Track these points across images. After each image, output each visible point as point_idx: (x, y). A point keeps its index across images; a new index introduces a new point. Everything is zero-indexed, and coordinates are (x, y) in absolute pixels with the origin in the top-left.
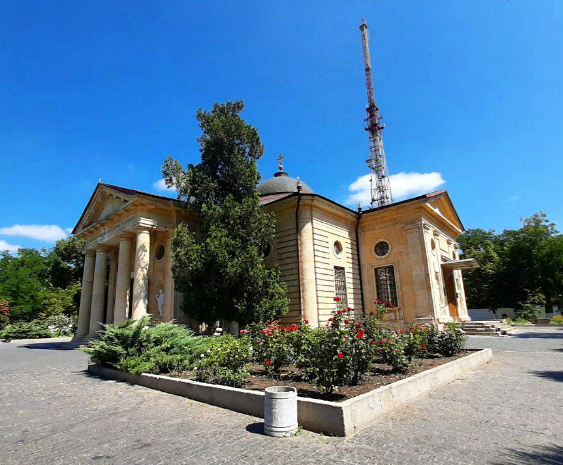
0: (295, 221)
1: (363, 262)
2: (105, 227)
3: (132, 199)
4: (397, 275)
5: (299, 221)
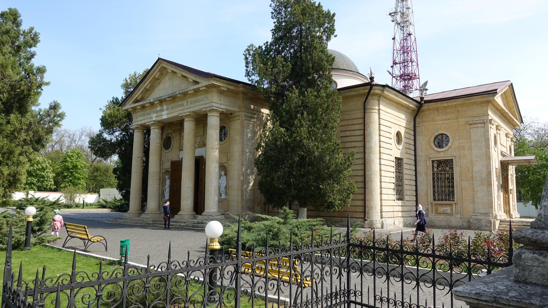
0: (363, 111)
1: (419, 153)
2: (163, 104)
3: (204, 83)
5: (366, 111)
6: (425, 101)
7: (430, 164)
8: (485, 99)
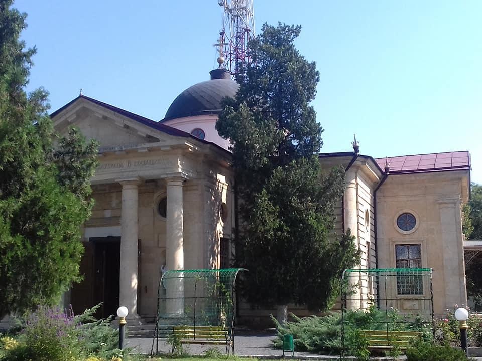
1: (379, 236)
4: (424, 256)
6: (390, 172)
7: (393, 249)
8: (457, 176)
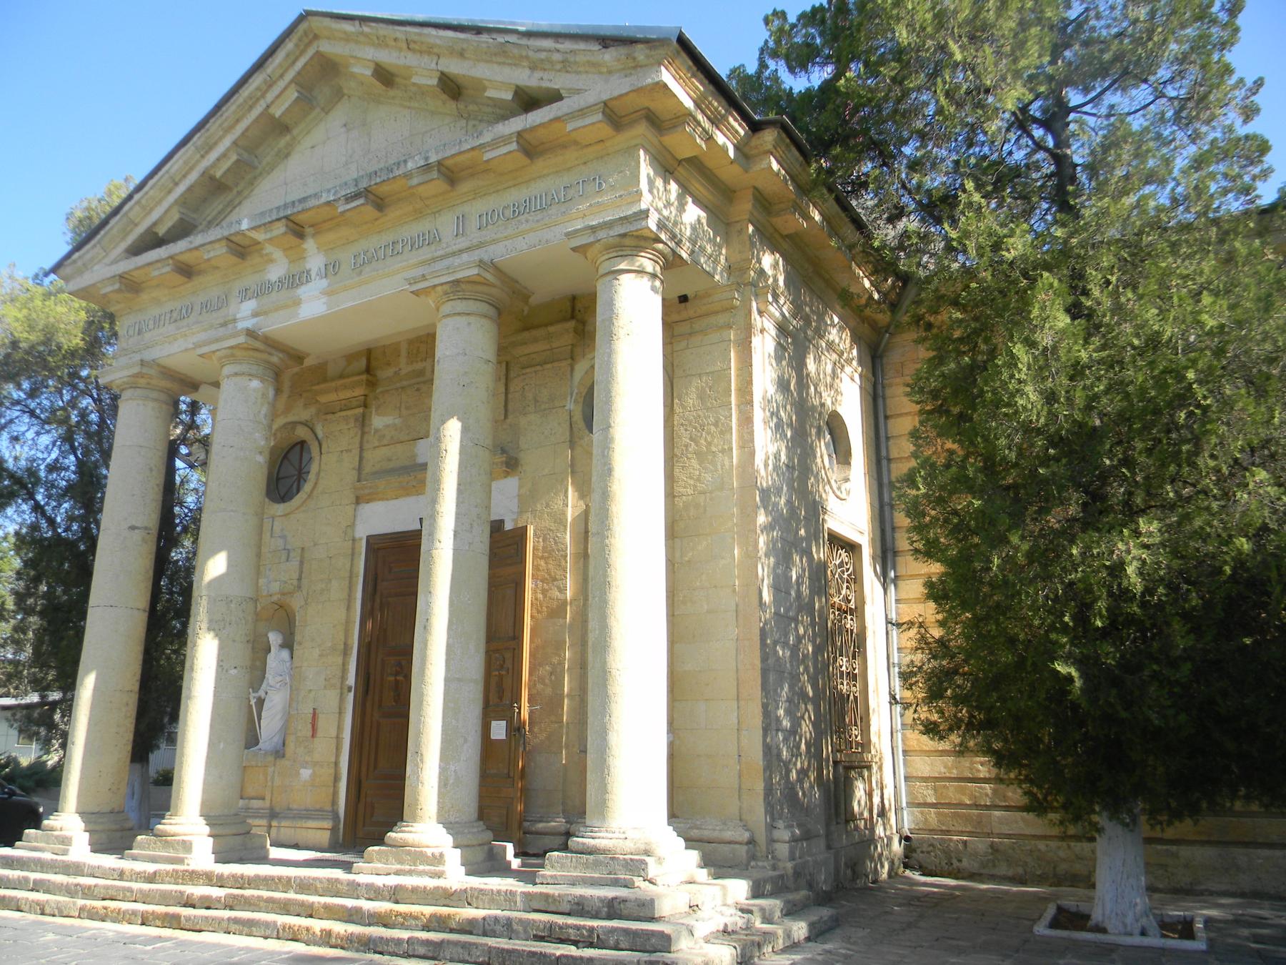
2: (310, 245)
